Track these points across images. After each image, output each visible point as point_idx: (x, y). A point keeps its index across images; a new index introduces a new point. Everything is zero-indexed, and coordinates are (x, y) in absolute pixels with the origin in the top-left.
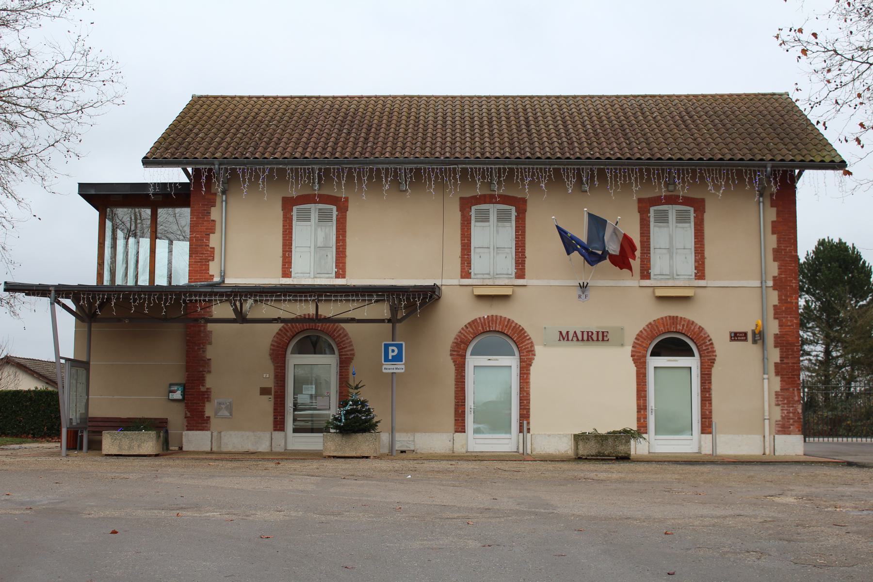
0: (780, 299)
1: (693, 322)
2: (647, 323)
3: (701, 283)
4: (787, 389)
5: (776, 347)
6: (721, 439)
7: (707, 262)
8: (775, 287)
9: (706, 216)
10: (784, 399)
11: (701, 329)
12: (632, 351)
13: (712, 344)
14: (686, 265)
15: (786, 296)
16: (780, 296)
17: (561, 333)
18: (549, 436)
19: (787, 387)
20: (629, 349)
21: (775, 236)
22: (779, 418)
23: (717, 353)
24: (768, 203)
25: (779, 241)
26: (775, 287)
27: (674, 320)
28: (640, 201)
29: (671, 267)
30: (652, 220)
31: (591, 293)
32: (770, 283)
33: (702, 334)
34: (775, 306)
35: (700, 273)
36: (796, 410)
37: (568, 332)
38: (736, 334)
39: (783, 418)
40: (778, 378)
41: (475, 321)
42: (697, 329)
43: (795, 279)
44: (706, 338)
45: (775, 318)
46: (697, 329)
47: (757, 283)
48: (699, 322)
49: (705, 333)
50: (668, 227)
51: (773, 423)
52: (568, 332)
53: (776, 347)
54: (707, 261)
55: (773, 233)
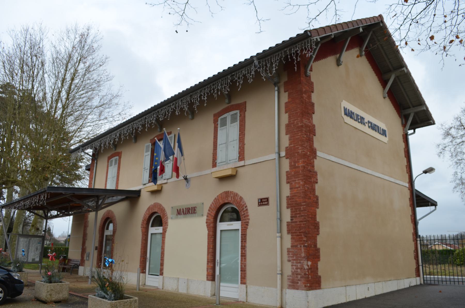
0: (291, 166)
1: (237, 194)
2: (214, 199)
3: (242, 163)
4: (296, 246)
5: (288, 208)
6: (252, 289)
7: (246, 147)
8: (287, 157)
9: (247, 113)
10: (294, 255)
11: (241, 198)
12: (207, 219)
13: (247, 210)
14: (234, 153)
15: (295, 162)
16: (290, 163)
17: (178, 210)
18: (170, 278)
19: (296, 244)
20: (205, 218)
21: (287, 114)
22: (290, 273)
23: (250, 217)
24: (282, 90)
25: (289, 117)
26: (287, 157)
27: (227, 193)
28: (215, 115)
29: (227, 155)
30: (219, 126)
31: (192, 182)
32: (283, 154)
33: (241, 203)
34: (287, 172)
35: (241, 157)
36: (302, 265)
37: (180, 210)
38: (261, 199)
39: (293, 273)
40: (289, 236)
41: (149, 207)
42: (239, 200)
43: (302, 145)
44: (244, 205)
45: (288, 183)
46: (239, 200)
47: (275, 156)
48: (241, 194)
49: (244, 202)
50: (226, 128)
51: (285, 278)
52: (180, 210)
53: (288, 208)
54: (246, 146)
55: (286, 112)
